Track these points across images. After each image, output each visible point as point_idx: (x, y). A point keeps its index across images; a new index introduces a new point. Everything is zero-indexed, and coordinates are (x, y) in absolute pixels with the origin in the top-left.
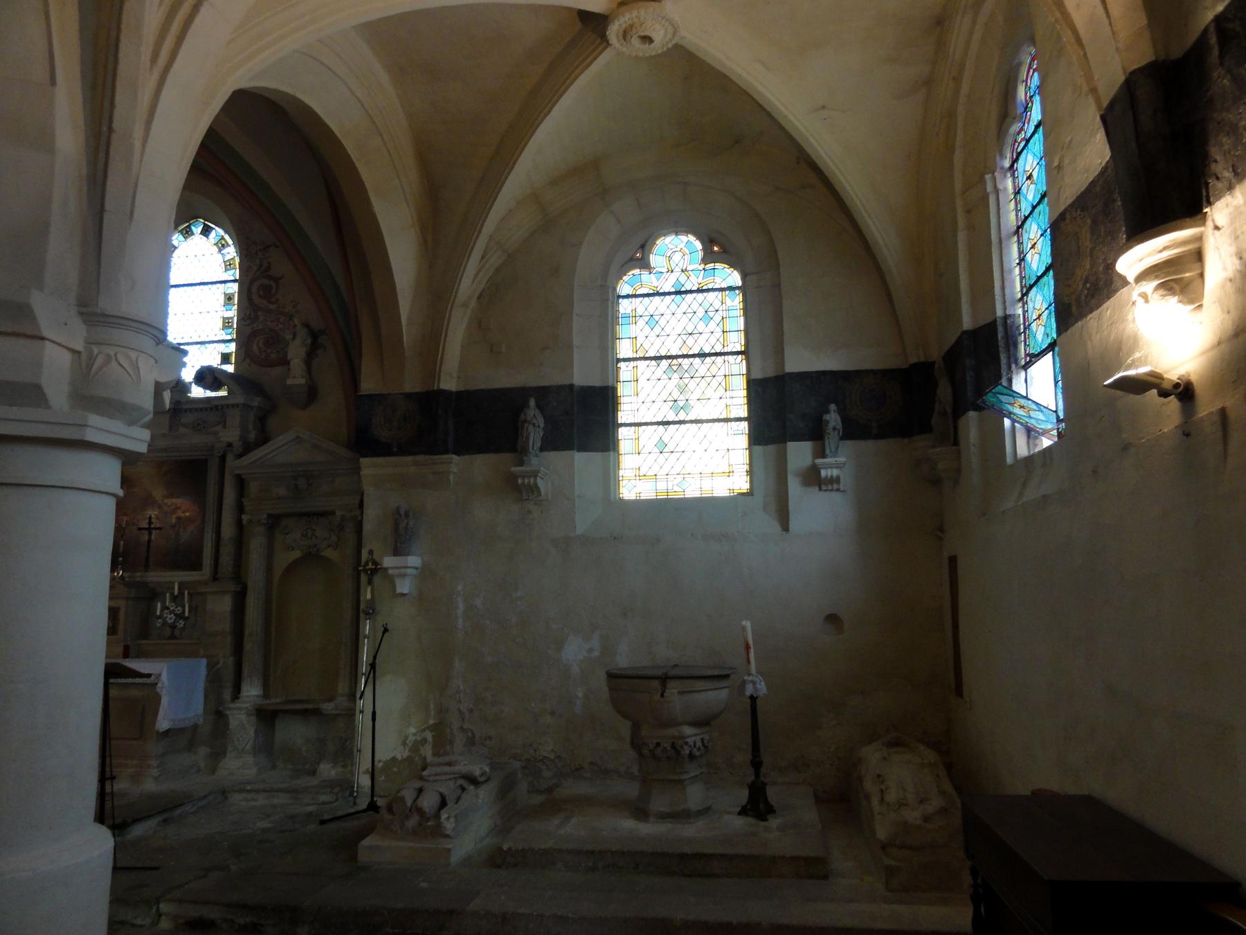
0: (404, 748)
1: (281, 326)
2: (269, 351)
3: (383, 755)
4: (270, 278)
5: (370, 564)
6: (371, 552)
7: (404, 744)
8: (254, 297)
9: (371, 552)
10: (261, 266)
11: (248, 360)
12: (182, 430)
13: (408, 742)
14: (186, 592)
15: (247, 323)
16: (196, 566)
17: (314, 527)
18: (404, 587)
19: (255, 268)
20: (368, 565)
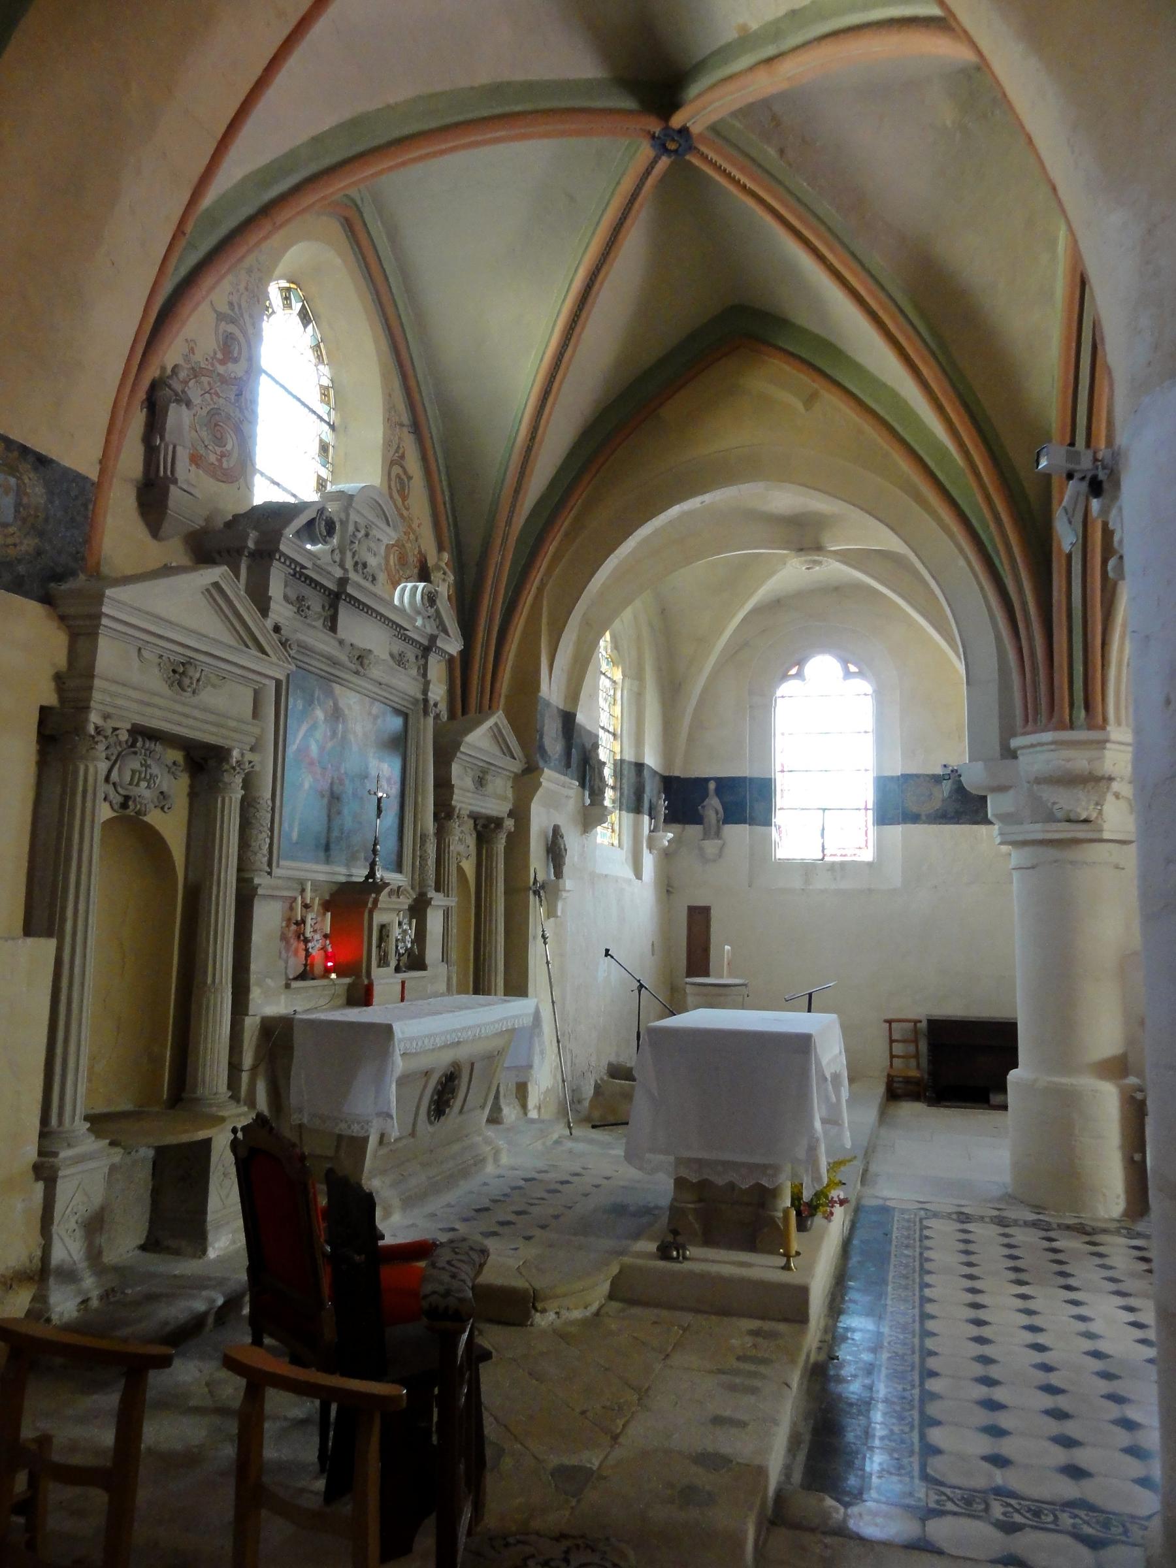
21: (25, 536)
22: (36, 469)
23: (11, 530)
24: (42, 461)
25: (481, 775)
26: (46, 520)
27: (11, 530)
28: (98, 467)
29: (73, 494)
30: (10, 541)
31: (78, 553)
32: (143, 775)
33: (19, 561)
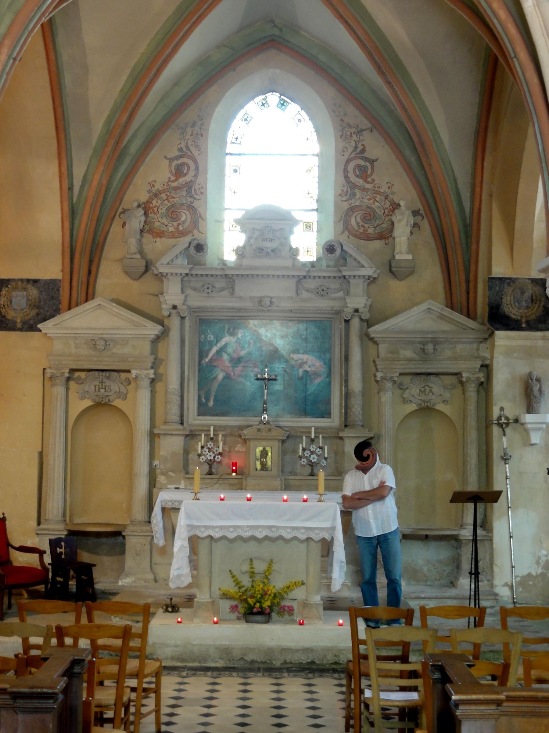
0: (538, 567)
1: (377, 204)
2: (366, 226)
3: (522, 571)
4: (366, 159)
5: (503, 418)
6: (502, 409)
7: (538, 563)
8: (351, 175)
9: (502, 409)
10: (356, 147)
11: (346, 233)
12: (305, 295)
13: (540, 561)
14: (321, 436)
15: (344, 199)
16: (326, 414)
17: (430, 385)
18: (536, 438)
19: (350, 149)
20: (501, 420)
21: (31, 310)
22: (33, 285)
23: (25, 310)
24: (35, 281)
25: (422, 347)
26: (40, 302)
27: (25, 310)
28: (61, 273)
29: (51, 288)
30: (25, 314)
31: (56, 308)
32: (100, 387)
33: (30, 320)
